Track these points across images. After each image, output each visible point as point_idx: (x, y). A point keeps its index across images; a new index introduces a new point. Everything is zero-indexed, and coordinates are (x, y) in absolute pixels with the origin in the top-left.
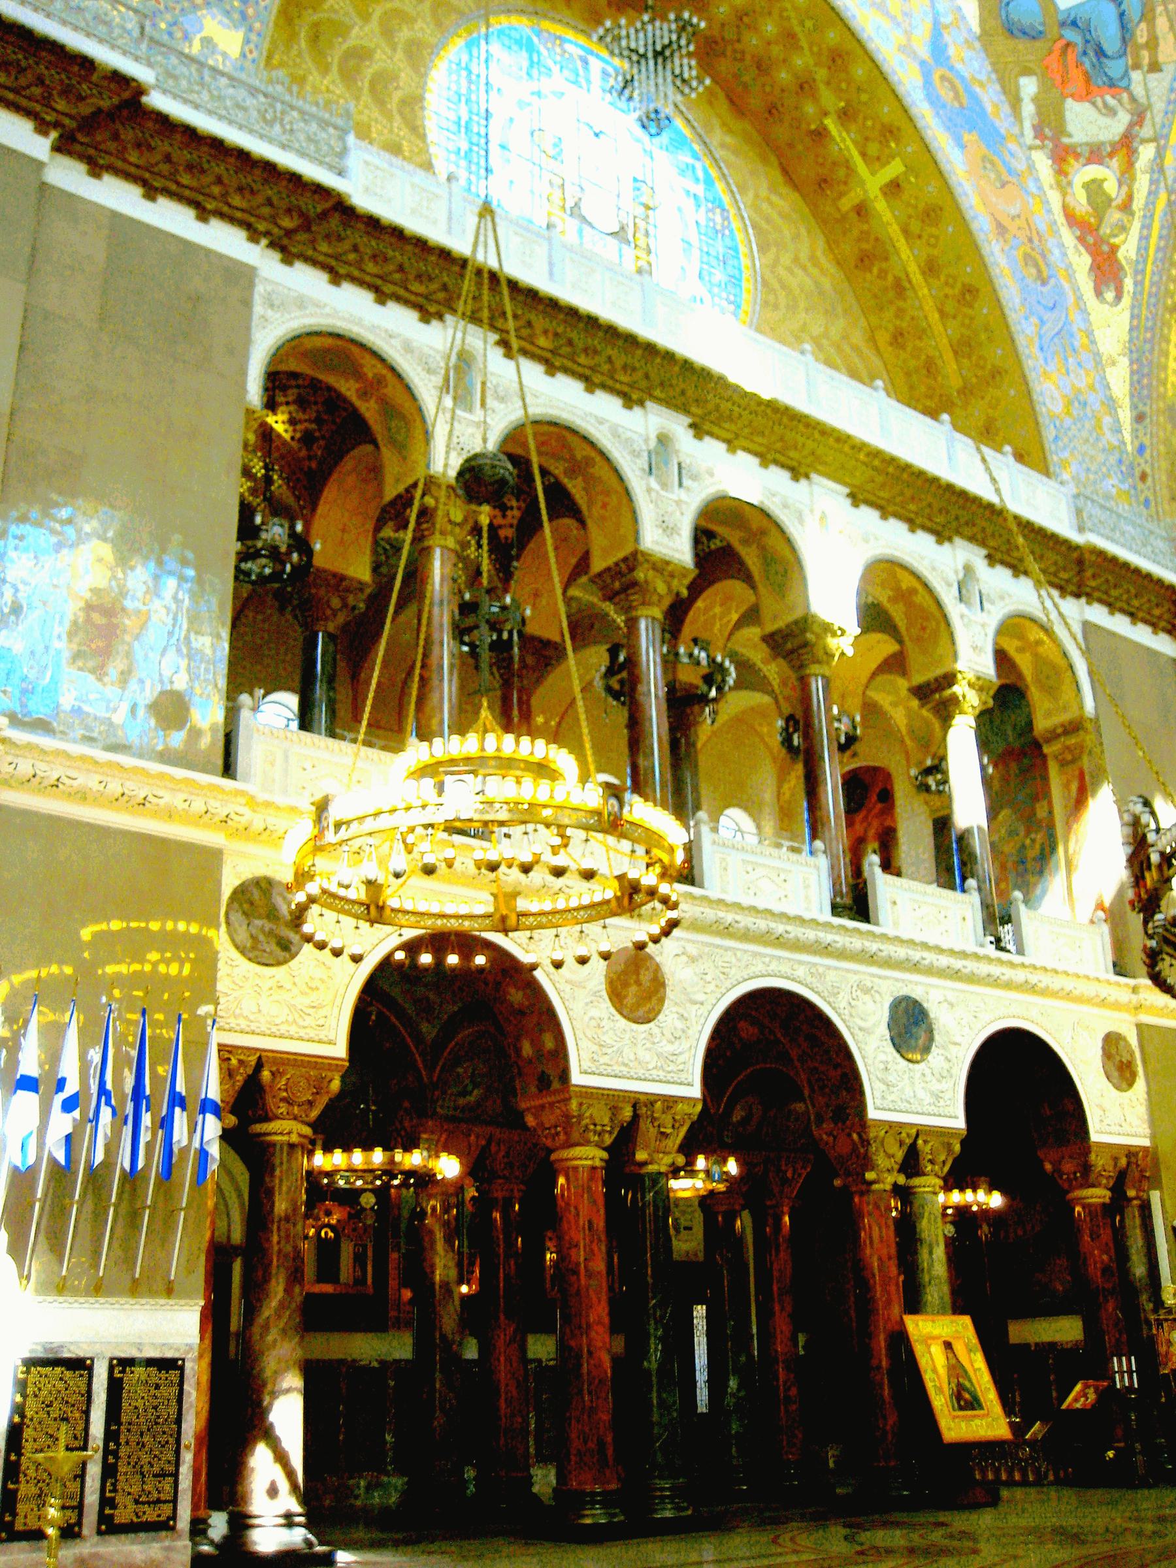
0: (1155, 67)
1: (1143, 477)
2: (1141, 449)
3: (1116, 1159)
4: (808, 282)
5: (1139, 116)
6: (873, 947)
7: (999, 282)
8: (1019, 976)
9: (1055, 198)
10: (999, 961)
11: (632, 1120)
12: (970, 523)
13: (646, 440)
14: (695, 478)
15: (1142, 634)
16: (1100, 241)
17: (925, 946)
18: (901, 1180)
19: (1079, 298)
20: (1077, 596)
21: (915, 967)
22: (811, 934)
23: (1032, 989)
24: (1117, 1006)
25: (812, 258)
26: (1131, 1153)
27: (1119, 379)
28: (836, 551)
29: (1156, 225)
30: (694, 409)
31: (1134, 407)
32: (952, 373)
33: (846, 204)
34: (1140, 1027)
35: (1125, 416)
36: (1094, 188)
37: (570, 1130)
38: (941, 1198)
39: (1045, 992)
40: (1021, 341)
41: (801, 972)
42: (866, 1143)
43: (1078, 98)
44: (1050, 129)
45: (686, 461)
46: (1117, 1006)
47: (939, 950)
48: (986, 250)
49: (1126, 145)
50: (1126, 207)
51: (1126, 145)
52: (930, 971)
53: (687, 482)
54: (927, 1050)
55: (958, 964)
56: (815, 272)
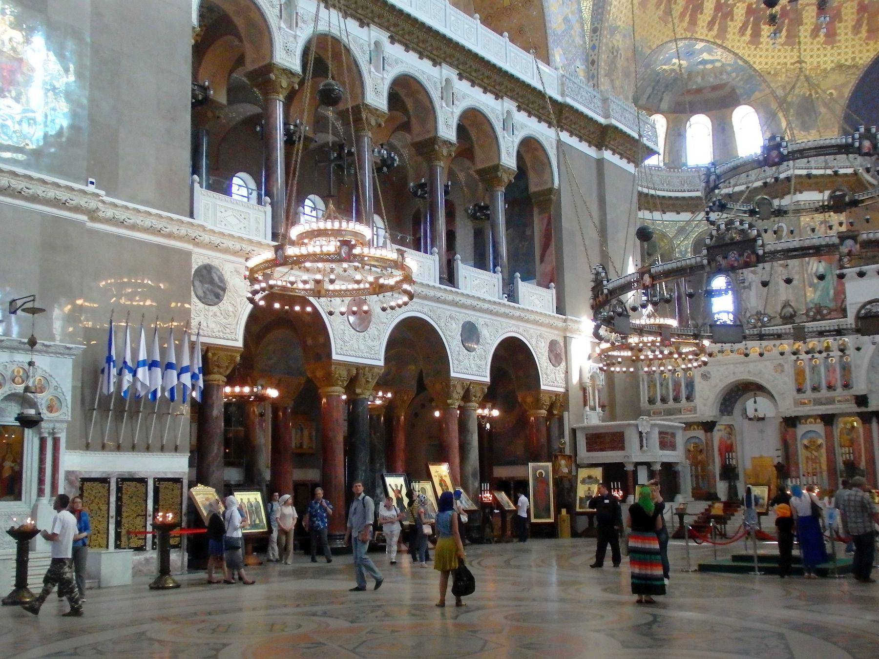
1: (593, 63)
2: (593, 48)
3: (550, 397)
6: (457, 299)
8: (517, 313)
10: (509, 306)
11: (356, 376)
12: (512, 90)
13: (369, 46)
14: (389, 65)
15: (583, 147)
17: (479, 298)
18: (462, 404)
21: (474, 308)
22: (432, 293)
23: (520, 319)
24: (556, 328)
26: (557, 394)
30: (392, 29)
31: (592, 23)
35: (588, 27)
37: (329, 379)
39: (527, 321)
41: (426, 310)
45: (386, 55)
46: (556, 328)
47: (484, 300)
55: (492, 307)
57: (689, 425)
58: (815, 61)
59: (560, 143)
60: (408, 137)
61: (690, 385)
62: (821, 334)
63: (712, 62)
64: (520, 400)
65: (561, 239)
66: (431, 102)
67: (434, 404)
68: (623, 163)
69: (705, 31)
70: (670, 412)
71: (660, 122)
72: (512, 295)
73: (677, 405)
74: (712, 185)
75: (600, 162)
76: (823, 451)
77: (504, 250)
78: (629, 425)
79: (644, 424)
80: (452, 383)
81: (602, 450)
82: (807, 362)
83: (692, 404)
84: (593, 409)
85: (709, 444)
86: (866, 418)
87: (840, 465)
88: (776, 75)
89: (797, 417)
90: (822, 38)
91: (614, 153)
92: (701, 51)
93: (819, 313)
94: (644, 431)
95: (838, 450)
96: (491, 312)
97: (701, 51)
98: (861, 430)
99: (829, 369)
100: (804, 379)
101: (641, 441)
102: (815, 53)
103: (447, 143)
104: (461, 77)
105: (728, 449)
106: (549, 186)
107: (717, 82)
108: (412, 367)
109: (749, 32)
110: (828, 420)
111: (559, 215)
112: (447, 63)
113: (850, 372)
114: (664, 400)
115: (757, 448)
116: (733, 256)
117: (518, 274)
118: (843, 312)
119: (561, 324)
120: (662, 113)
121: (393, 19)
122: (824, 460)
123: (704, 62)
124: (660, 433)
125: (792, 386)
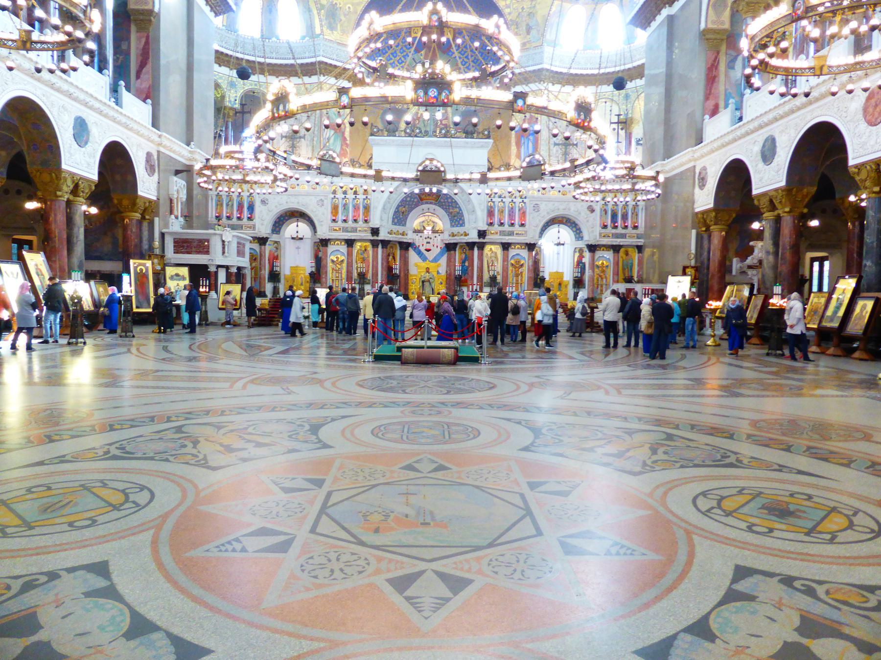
18: (71, 197)
26: (150, 201)
34: (158, 152)
38: (84, 208)
39: (131, 129)
42: (58, 178)
46: (152, 141)
54: (86, 143)
55: (103, 108)
61: (251, 208)
64: (116, 201)
72: (118, 102)
73: (240, 222)
76: (345, 265)
78: (215, 234)
80: (63, 175)
82: (340, 200)
83: (251, 223)
85: (262, 255)
86: (375, 244)
87: (355, 275)
95: (355, 266)
96: (101, 113)
98: (371, 252)
101: (224, 248)
105: (274, 258)
110: (350, 243)
114: (228, 218)
115: (296, 259)
119: (157, 139)
122: (344, 271)
124: (238, 243)
125: (329, 217)
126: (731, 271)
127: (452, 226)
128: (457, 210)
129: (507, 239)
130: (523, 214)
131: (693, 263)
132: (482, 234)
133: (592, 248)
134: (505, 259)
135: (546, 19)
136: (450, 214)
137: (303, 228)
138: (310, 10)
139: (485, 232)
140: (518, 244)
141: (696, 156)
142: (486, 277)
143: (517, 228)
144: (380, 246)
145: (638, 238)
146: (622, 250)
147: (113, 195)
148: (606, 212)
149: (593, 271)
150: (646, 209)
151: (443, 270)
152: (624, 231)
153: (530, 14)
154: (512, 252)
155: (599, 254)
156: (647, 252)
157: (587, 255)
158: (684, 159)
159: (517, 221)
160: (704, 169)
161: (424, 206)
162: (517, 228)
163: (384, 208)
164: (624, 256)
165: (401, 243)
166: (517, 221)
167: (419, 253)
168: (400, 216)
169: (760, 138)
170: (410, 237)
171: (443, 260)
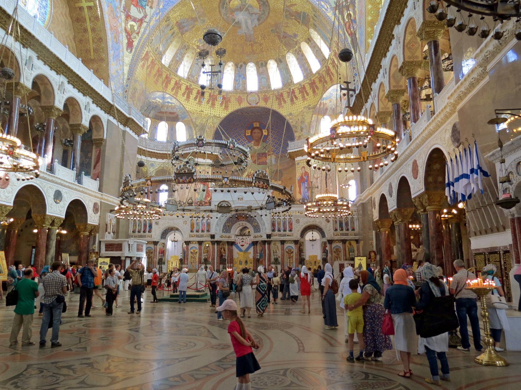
0: (151, 7)
1: (126, 91)
2: (127, 86)
4: (63, 20)
5: (145, 16)
6: (54, 179)
7: (108, 40)
8: (81, 189)
9: (123, 24)
13: (26, 57)
14: (35, 69)
16: (130, 38)
17: (64, 181)
18: (50, 227)
19: (123, 49)
20: (108, 114)
21: (62, 185)
24: (98, 197)
25: (65, 14)
26: (95, 226)
27: (126, 69)
28: (63, 92)
29: (142, 41)
32: (92, 55)
33: (77, 5)
34: (101, 202)
35: (126, 77)
36: (132, 26)
39: (86, 193)
40: (109, 55)
42: (44, 218)
43: (135, 6)
44: (127, 10)
45: (34, 64)
46: (98, 197)
47: (67, 182)
48: (107, 31)
49: (141, 21)
50: (138, 33)
51: (141, 21)
52: (65, 186)
53: (33, 69)
55: (70, 185)
56: (65, 17)
57: (149, 242)
58: (207, 112)
59: (108, 120)
60: (37, 103)
61: (150, 226)
62: (205, 211)
63: (171, 103)
64: (77, 227)
65: (104, 159)
66: (53, 90)
67: (36, 226)
68: (133, 134)
69: (170, 91)
70: (141, 236)
71: (149, 121)
72: (80, 181)
73: (145, 234)
74: (176, 150)
75: (124, 132)
76: (198, 255)
77: (78, 160)
78: (125, 241)
79: (131, 241)
81: (112, 251)
83: (150, 234)
84: (109, 233)
86: (213, 243)
87: (203, 261)
88: (193, 113)
89: (190, 241)
90: (210, 105)
91: (130, 129)
92: (168, 98)
93: (201, 204)
94: (131, 244)
96: (69, 187)
97: (168, 98)
99: (203, 224)
100: (194, 227)
101: (129, 248)
102: (207, 109)
103: (58, 109)
104: (69, 82)
106: (102, 137)
107: (172, 111)
108: (25, 208)
109: (186, 96)
110: (200, 243)
111: (105, 151)
112: (63, 75)
113: (210, 225)
116: (184, 178)
117: (83, 172)
118: (210, 203)
119: (100, 196)
120: (150, 118)
121: (40, 49)
122: (197, 258)
123: (168, 102)
124: (137, 245)
126: (394, 254)
127: (255, 232)
128: (256, 224)
129: (282, 238)
130: (291, 224)
131: (375, 249)
132: (269, 236)
133: (330, 242)
134: (283, 249)
135: (310, 124)
136: (253, 226)
137: (178, 236)
138: (191, 128)
139: (270, 235)
140: (290, 241)
141: (371, 191)
142: (272, 260)
143: (287, 232)
144: (216, 244)
145: (355, 235)
146: (347, 242)
147: (76, 224)
148: (336, 223)
149: (332, 255)
150: (358, 219)
151: (251, 256)
152: (347, 232)
153: (302, 122)
154: (286, 245)
155: (334, 245)
156: (361, 243)
157: (328, 245)
158: (366, 194)
159: (288, 229)
160: (374, 199)
161: (240, 222)
162: (287, 232)
163: (217, 224)
164: (349, 246)
165: (228, 242)
166: (288, 229)
167: (238, 247)
168: (227, 228)
169: (387, 183)
170: (232, 239)
171: (251, 250)
